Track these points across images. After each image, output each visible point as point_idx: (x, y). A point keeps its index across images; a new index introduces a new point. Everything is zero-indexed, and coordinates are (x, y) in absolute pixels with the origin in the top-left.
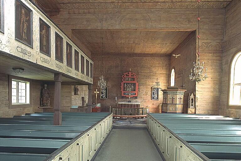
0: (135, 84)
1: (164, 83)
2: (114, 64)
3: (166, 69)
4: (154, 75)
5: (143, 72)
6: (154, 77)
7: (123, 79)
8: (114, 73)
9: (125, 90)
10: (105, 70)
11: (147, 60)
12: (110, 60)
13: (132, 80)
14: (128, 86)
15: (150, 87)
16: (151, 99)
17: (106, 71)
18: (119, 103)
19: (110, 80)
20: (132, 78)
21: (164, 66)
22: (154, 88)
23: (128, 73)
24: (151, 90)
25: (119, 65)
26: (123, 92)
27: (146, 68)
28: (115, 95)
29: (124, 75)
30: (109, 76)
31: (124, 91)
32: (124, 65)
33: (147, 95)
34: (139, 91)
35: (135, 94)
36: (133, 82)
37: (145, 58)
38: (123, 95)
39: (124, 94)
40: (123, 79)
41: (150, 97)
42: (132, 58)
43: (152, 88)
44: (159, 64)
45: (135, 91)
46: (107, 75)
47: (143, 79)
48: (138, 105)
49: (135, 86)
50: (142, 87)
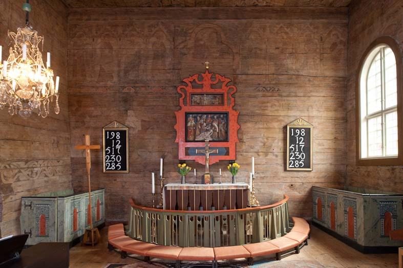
0: (226, 114)
1: (327, 109)
2: (150, 47)
3: (335, 59)
4: (290, 81)
5: (251, 72)
6: (292, 89)
7: (181, 100)
8: (149, 78)
9: (191, 138)
10: (116, 69)
11: (264, 29)
12: (133, 35)
13: (217, 101)
14: (201, 125)
15: (277, 126)
16: (285, 170)
17: (122, 74)
18: (171, 186)
19: (135, 103)
20: (215, 95)
21: (329, 51)
22: (295, 129)
23: (202, 79)
24: (281, 136)
25: (168, 51)
26: (183, 146)
27: (265, 58)
28: (155, 156)
29: (187, 85)
30: (133, 90)
31: (187, 141)
32: (185, 51)
33: (270, 156)
34: (241, 140)
35: (227, 153)
36: (220, 109)
37: (256, 24)
38: (182, 156)
39: (187, 154)
40: (181, 100)
41: (280, 161)
42: (212, 26)
43: (285, 127)
44: (309, 41)
45: (226, 140)
46: (124, 87)
47: (255, 97)
48: (240, 197)
49: (227, 123)
50: (249, 125)
